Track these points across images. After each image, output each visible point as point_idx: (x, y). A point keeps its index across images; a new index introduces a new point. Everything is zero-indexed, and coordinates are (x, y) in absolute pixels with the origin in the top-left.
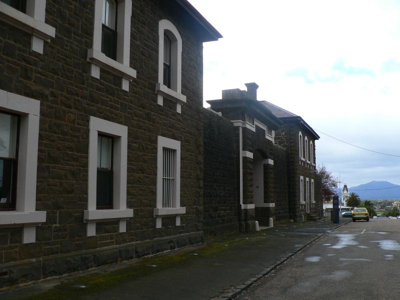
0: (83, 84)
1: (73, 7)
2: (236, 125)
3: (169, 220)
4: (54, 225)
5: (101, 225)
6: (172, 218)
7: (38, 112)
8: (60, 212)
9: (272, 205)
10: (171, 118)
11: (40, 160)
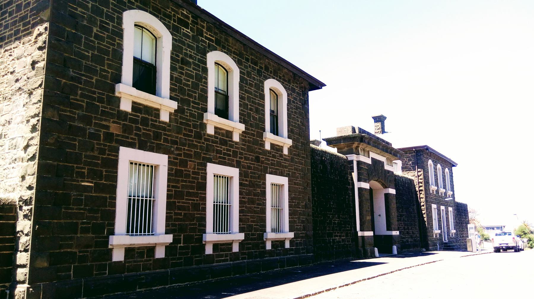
0: (201, 139)
1: (190, 83)
2: (349, 159)
3: (278, 244)
4: (179, 245)
5: (216, 246)
6: (282, 242)
7: (166, 163)
8: (184, 235)
9: (396, 233)
10: (278, 159)
11: (169, 197)
